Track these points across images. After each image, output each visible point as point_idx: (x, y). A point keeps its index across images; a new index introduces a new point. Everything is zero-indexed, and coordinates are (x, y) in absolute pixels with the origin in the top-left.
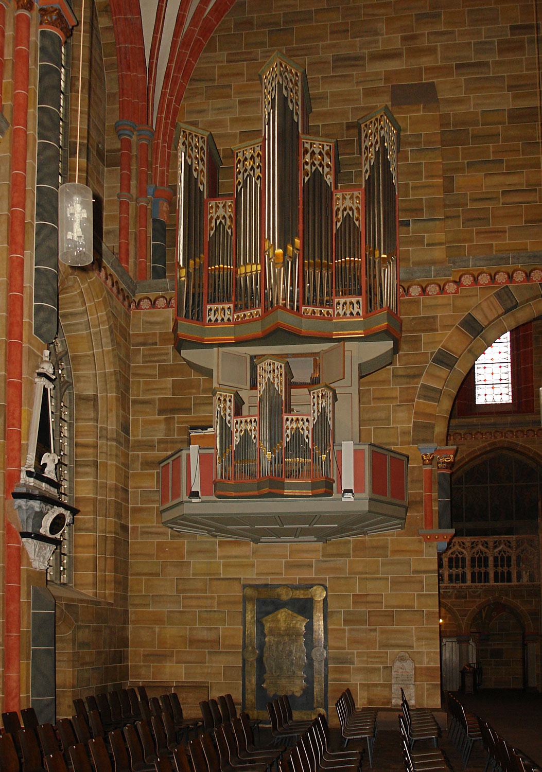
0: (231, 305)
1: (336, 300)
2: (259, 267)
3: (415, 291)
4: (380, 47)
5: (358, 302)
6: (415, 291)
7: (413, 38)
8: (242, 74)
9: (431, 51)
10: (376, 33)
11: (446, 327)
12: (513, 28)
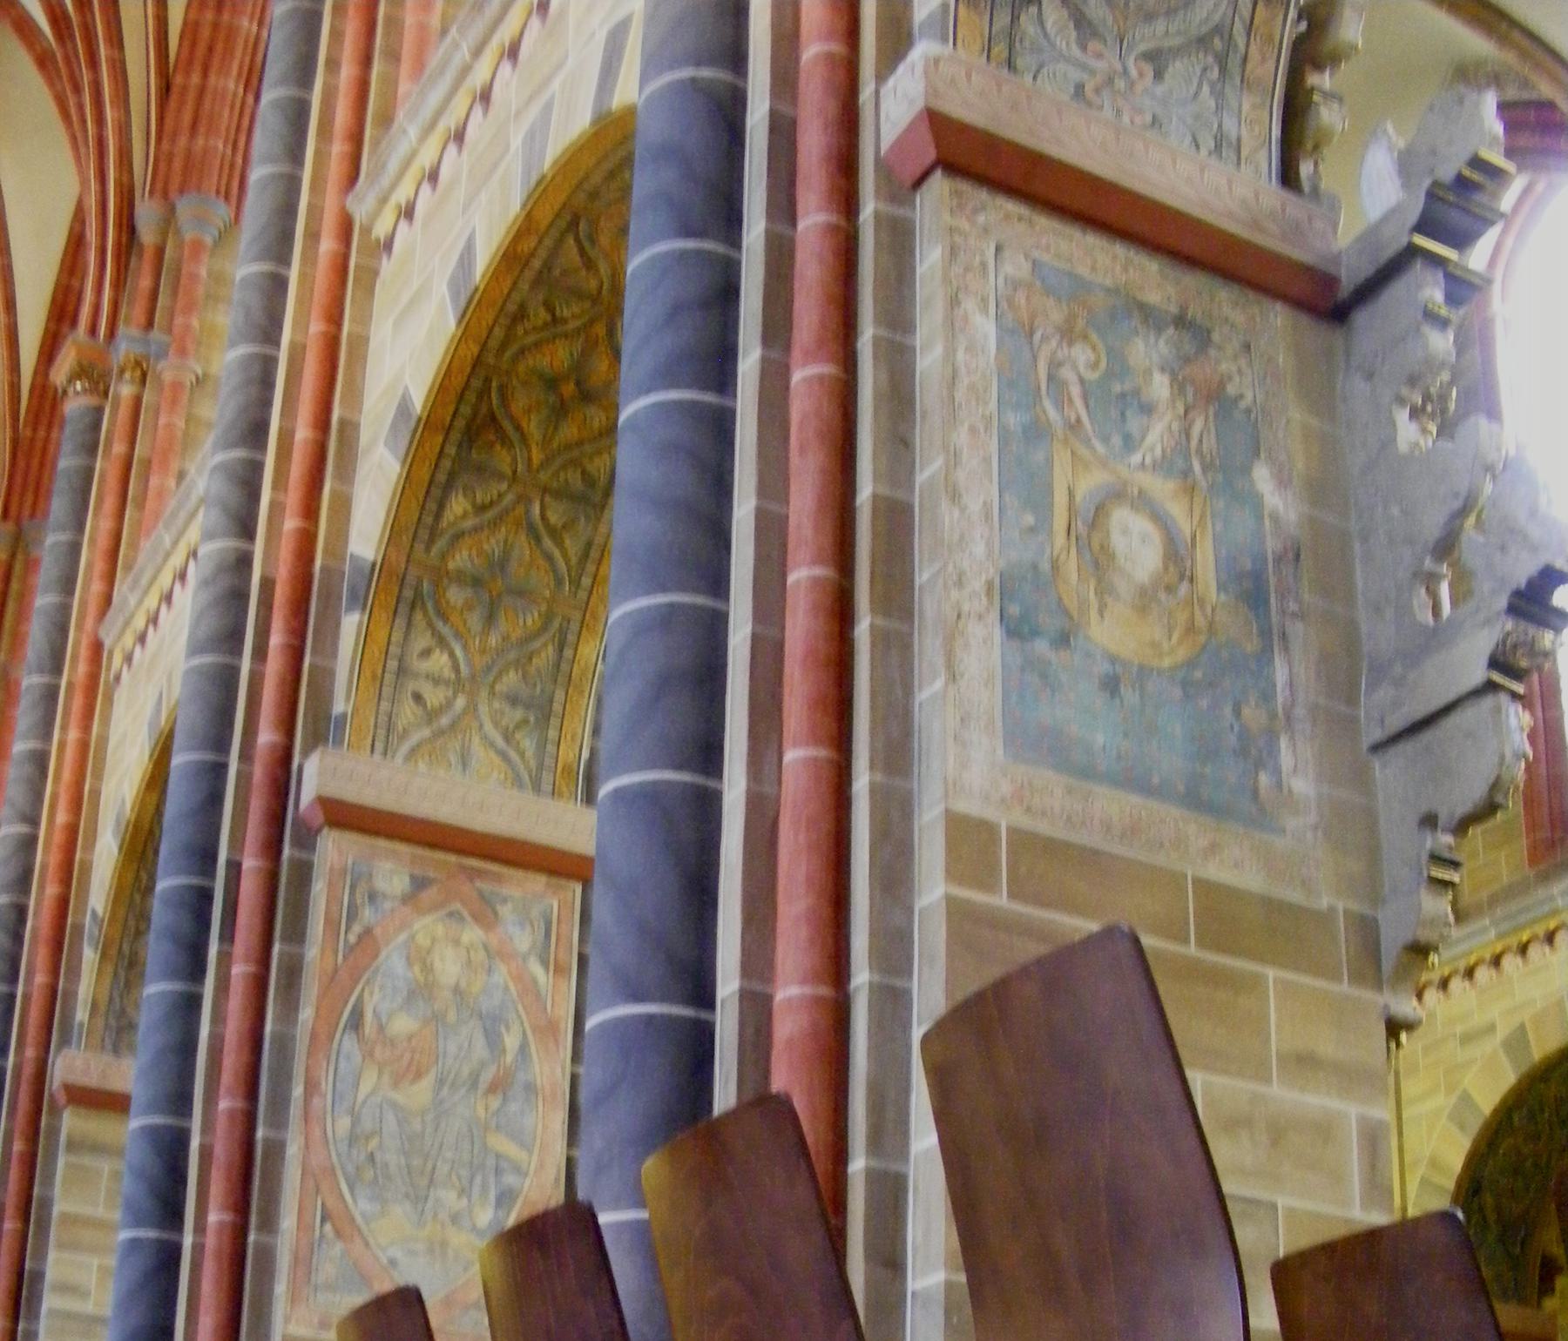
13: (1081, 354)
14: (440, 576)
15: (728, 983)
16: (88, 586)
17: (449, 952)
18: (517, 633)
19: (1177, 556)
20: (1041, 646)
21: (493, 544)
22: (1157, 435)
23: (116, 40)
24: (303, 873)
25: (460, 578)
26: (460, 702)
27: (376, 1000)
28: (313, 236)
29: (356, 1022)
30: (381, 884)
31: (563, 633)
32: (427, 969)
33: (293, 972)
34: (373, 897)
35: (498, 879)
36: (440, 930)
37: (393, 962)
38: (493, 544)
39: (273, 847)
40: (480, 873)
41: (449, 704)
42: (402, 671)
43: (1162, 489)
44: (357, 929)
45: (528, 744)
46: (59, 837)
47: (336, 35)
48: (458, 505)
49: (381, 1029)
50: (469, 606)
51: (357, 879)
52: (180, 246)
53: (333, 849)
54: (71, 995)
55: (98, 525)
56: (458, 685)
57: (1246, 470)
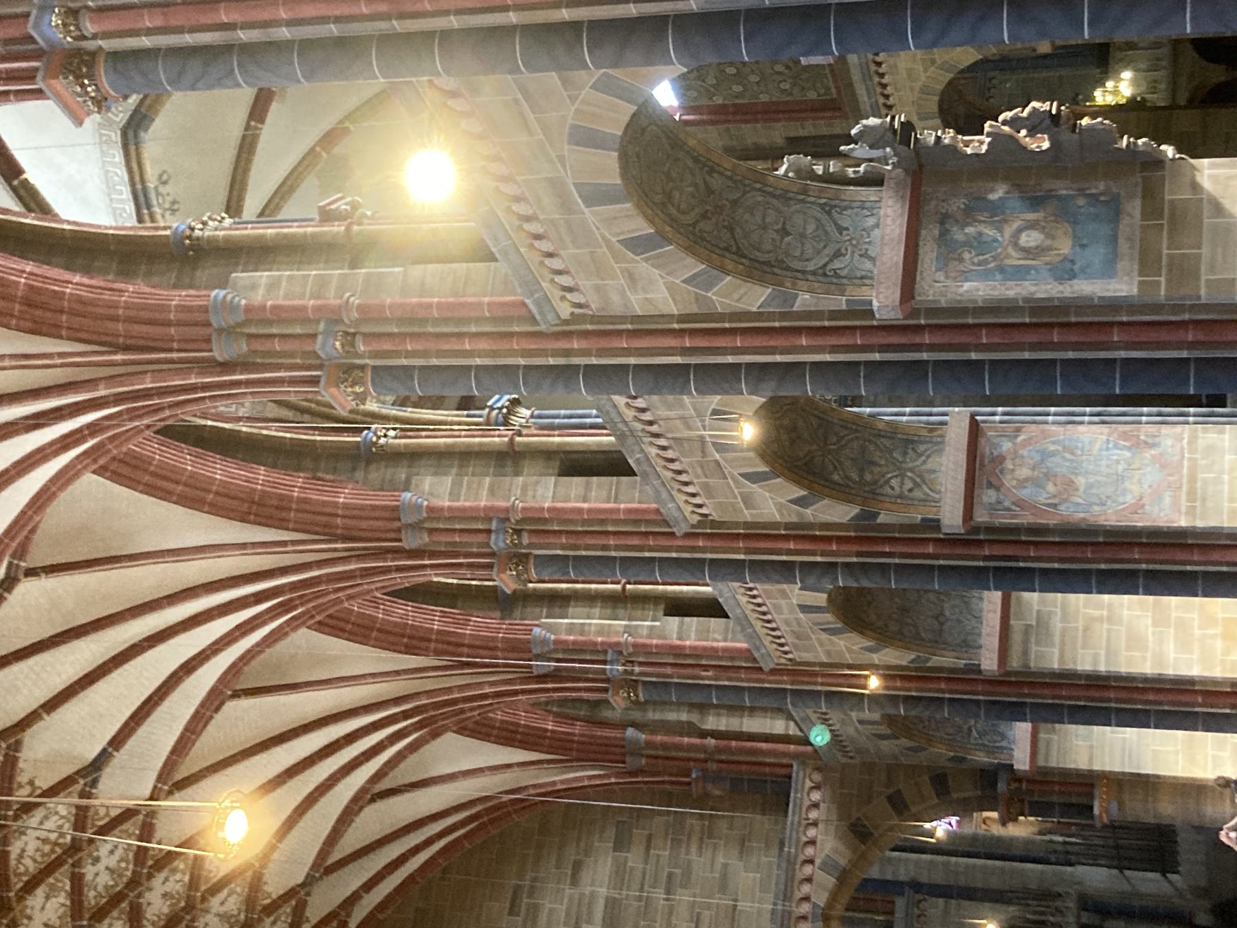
12: (511, 913)
13: (967, 256)
14: (862, 483)
15: (1184, 354)
17: (1017, 472)
18: (878, 453)
19: (1031, 226)
20: (1076, 268)
21: (848, 463)
22: (989, 232)
23: (449, 690)
24: (990, 529)
25: (861, 477)
26: (909, 474)
27: (1042, 498)
28: (693, 549)
29: (1055, 506)
30: (993, 500)
31: (874, 436)
32: (1026, 480)
34: (999, 503)
35: (983, 456)
36: (1009, 477)
37: (1025, 493)
38: (848, 463)
39: (979, 543)
40: (982, 461)
41: (911, 478)
42: (901, 496)
43: (1008, 231)
44: (1013, 507)
45: (922, 448)
47: (587, 548)
48: (836, 477)
49: (1054, 496)
50: (871, 472)
51: (993, 508)
52: (556, 651)
53: (981, 517)
56: (902, 476)
57: (990, 201)
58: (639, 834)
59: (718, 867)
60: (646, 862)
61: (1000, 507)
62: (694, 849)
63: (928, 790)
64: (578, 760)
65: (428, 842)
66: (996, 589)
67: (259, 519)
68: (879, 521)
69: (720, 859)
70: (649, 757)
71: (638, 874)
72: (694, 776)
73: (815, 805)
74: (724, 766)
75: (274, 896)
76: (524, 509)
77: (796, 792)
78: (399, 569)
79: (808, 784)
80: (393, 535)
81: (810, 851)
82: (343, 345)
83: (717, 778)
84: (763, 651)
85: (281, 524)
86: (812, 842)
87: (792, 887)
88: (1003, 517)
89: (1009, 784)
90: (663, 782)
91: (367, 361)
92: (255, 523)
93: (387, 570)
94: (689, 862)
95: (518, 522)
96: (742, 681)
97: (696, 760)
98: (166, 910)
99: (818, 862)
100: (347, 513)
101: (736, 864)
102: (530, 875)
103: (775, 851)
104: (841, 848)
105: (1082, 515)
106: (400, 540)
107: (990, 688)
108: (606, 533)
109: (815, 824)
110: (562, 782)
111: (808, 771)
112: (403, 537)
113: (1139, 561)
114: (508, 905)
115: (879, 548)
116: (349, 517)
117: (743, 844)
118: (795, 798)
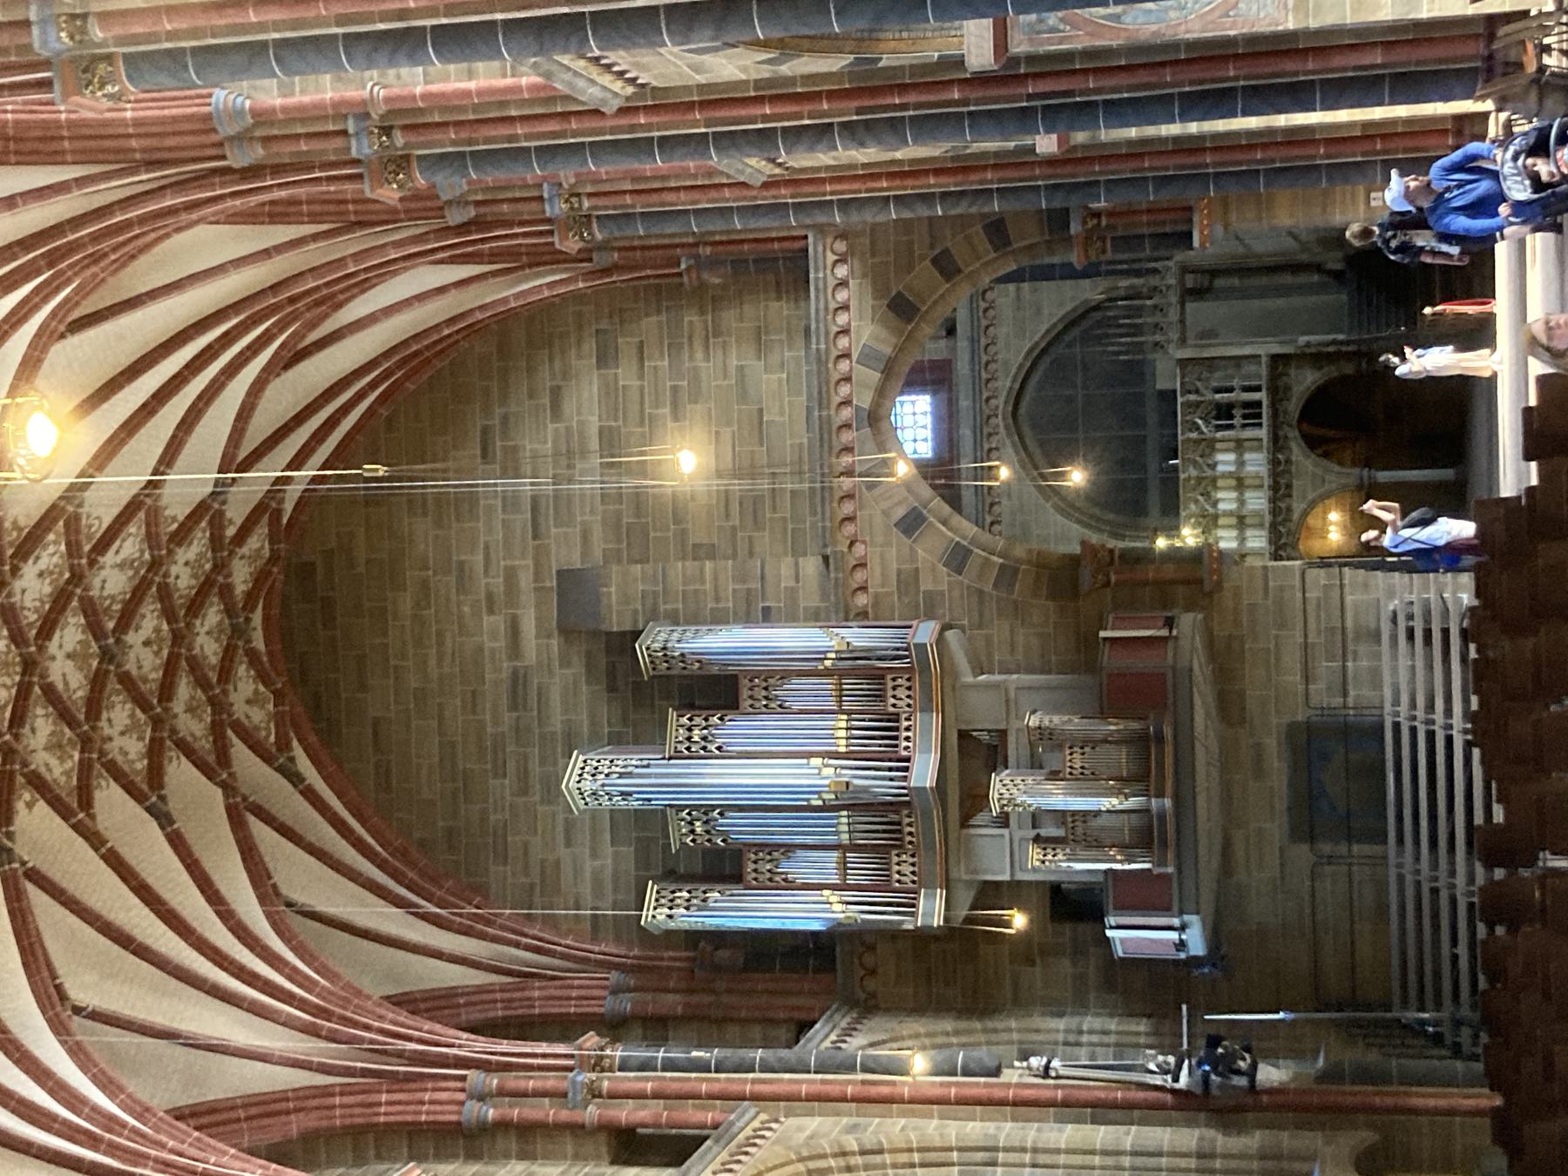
0: (894, 852)
1: (891, 709)
2: (845, 813)
3: (862, 600)
4: (501, 643)
5: (894, 679)
6: (862, 600)
7: (490, 598)
8: (526, 845)
9: (511, 575)
10: (480, 649)
11: (913, 555)
16: (729, 199)
24: (1031, 59)
28: (633, 128)
33: (1088, 54)
46: (897, 182)
54: (996, 154)
55: (683, 202)
58: (626, 344)
59: (733, 371)
60: (641, 377)
61: (1043, 27)
62: (699, 355)
63: (983, 243)
64: (530, 266)
65: (360, 396)
66: (1047, 132)
67: (20, 158)
68: (881, 65)
69: (734, 362)
70: (620, 249)
71: (634, 396)
72: (683, 266)
73: (843, 284)
74: (720, 248)
75: (181, 518)
76: (388, 100)
77: (817, 271)
78: (234, 195)
79: (831, 258)
80: (213, 152)
81: (843, 342)
82: (72, 38)
83: (713, 263)
84: (749, 170)
85: (54, 158)
86: (845, 331)
87: (828, 391)
88: (1049, 41)
89: (1084, 223)
90: (648, 277)
91: (113, 50)
92: (18, 163)
93: (221, 198)
94: (696, 369)
95: (382, 117)
96: (727, 200)
97: (682, 245)
98: (47, 589)
99: (855, 356)
100: (142, 130)
101: (754, 365)
102: (498, 411)
103: (800, 342)
104: (884, 334)
105: (1154, 28)
106: (223, 157)
107: (1050, 171)
108: (511, 119)
109: (845, 307)
110: (517, 296)
111: (829, 240)
112: (228, 154)
113: (1236, 78)
114: (478, 452)
115: (888, 101)
116: (147, 135)
117: (760, 340)
118: (817, 279)
